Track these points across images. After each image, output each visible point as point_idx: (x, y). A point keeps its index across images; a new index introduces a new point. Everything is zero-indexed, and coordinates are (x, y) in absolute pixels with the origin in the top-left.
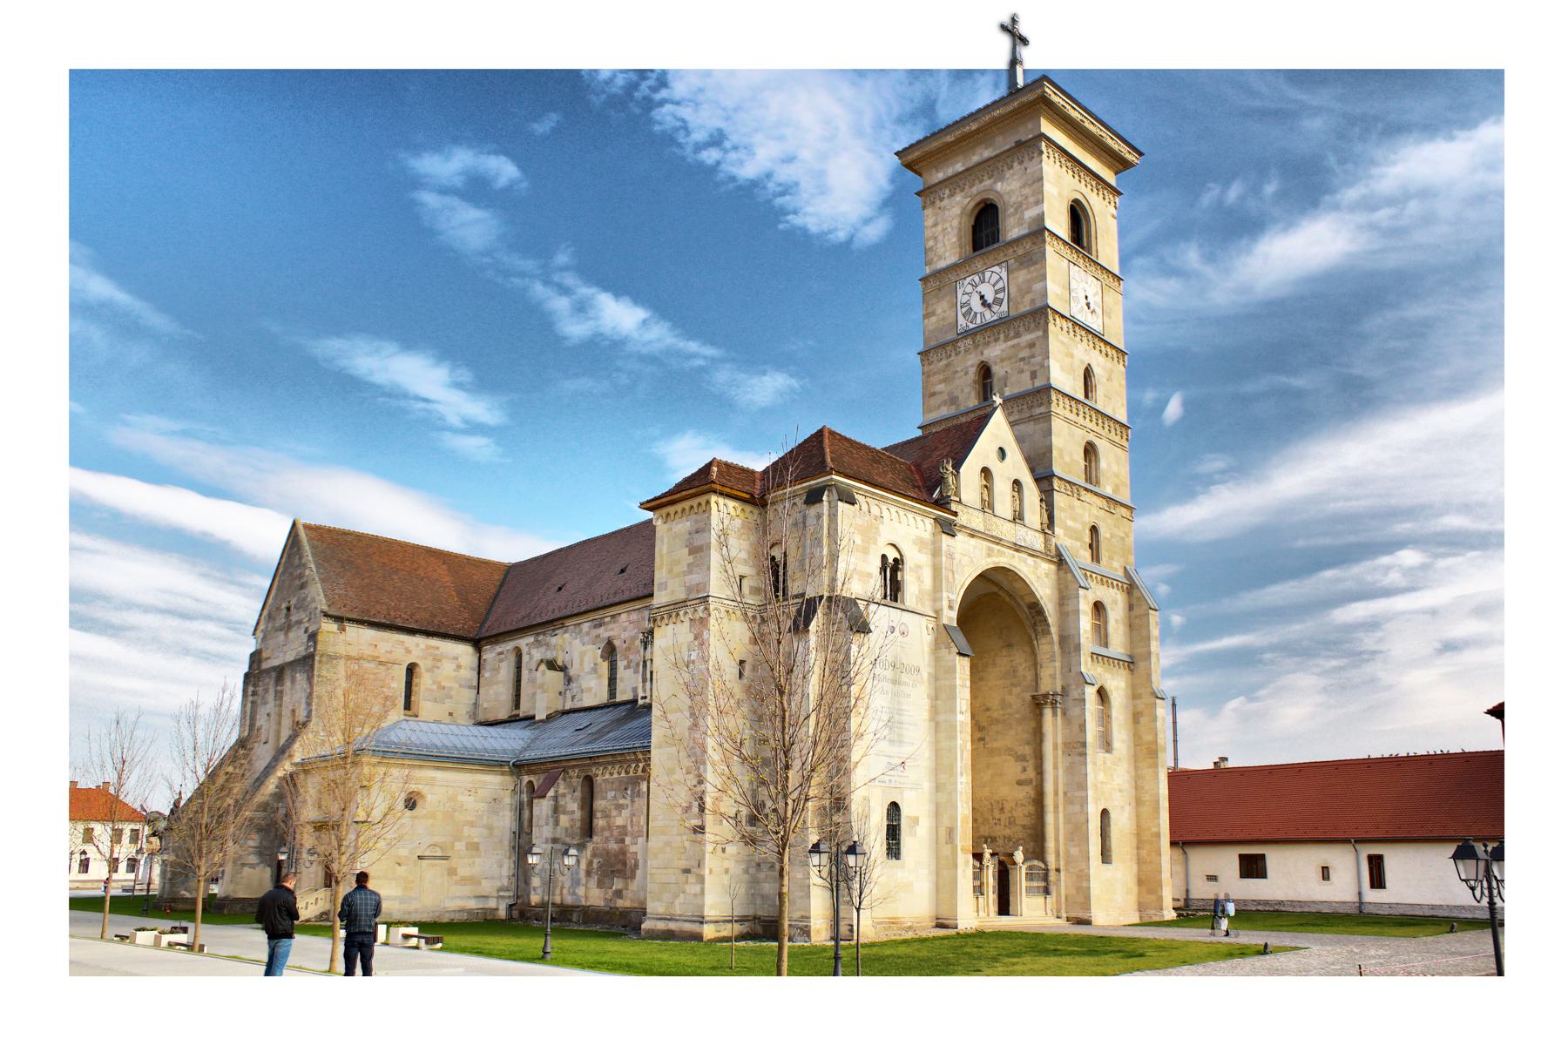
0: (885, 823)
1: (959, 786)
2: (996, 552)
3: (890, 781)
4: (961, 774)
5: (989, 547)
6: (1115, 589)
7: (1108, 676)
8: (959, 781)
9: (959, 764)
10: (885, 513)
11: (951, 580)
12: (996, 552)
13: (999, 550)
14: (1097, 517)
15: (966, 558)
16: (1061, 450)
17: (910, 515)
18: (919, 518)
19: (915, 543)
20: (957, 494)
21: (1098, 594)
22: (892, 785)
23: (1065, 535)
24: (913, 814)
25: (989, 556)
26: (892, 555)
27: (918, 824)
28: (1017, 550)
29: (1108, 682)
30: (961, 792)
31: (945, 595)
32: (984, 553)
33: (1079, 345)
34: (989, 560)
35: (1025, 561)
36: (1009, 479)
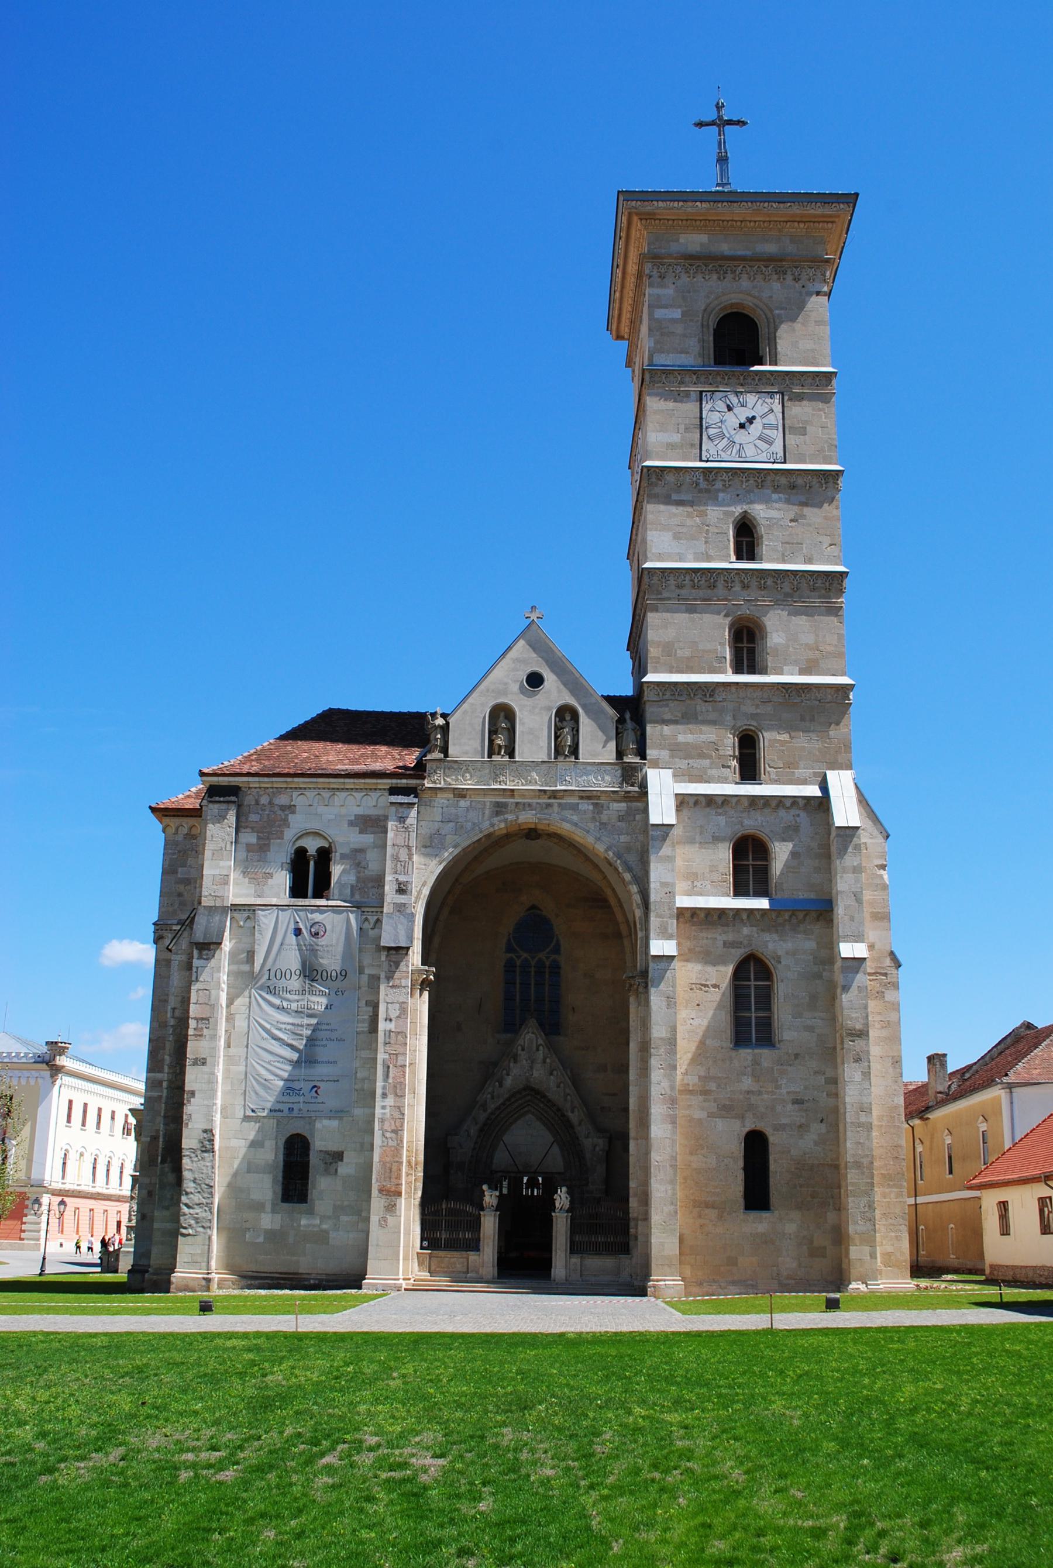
0: (281, 1157)
1: (378, 1111)
2: (511, 807)
3: (291, 1110)
4: (384, 1095)
5: (497, 803)
6: (793, 812)
7: (767, 937)
8: (379, 1102)
9: (379, 1084)
10: (299, 800)
11: (403, 855)
12: (513, 807)
13: (517, 803)
14: (754, 716)
15: (451, 825)
16: (668, 649)
17: (344, 794)
18: (358, 795)
19: (351, 824)
20: (445, 750)
21: (746, 822)
22: (295, 1113)
23: (672, 756)
24: (334, 1147)
25: (498, 814)
26: (312, 846)
27: (342, 1160)
28: (555, 798)
29: (771, 946)
30: (382, 1121)
31: (389, 878)
32: (487, 812)
33: (721, 495)
34: (495, 820)
35: (574, 808)
36: (549, 709)
